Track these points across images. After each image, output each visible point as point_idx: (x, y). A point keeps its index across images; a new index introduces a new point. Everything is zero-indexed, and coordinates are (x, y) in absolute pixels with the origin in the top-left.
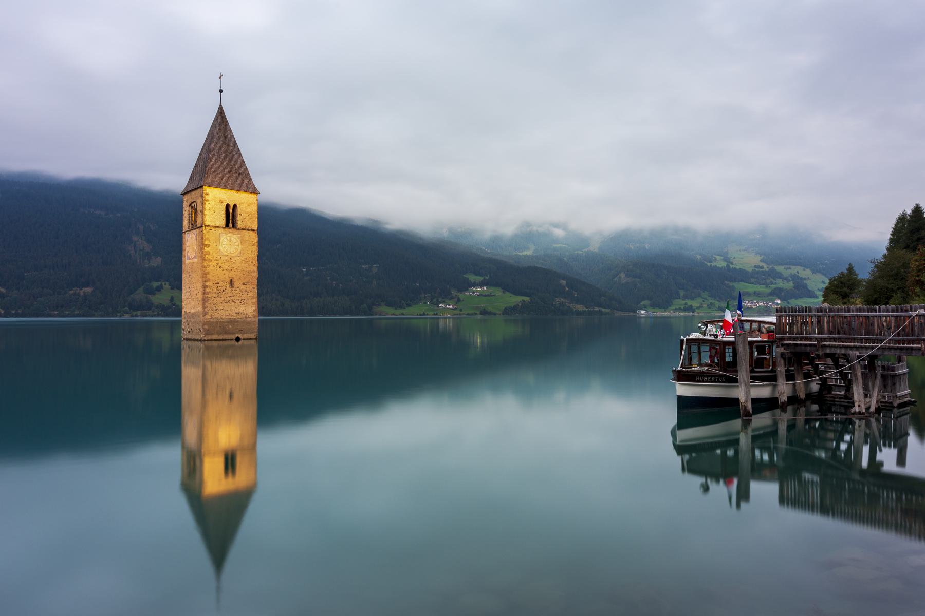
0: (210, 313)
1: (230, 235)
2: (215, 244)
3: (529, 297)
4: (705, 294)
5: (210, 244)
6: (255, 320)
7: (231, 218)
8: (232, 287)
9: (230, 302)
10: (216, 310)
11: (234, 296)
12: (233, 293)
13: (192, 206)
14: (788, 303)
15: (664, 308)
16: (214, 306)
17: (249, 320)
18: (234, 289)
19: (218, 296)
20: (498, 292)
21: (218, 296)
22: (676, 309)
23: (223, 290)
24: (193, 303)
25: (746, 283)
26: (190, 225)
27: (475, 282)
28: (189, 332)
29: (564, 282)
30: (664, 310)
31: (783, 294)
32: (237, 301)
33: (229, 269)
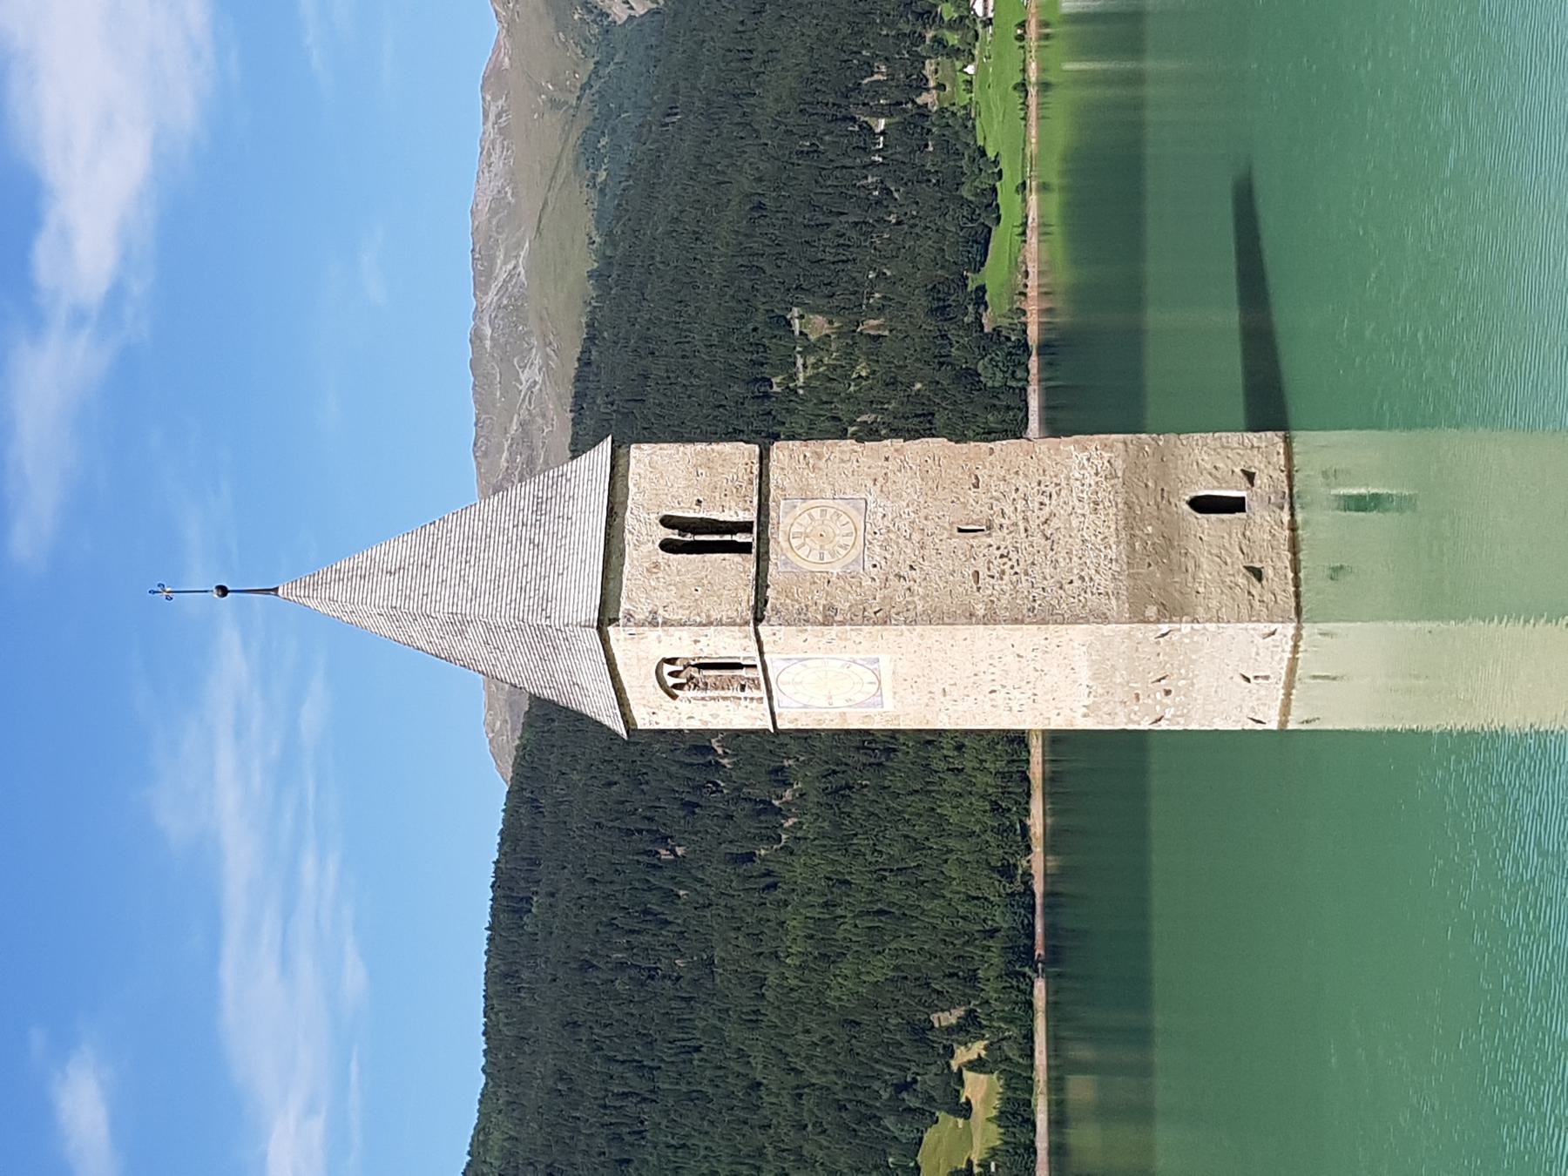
0: (1094, 601)
2: (822, 584)
5: (823, 602)
6: (1121, 446)
7: (716, 538)
8: (989, 528)
9: (1048, 534)
10: (1082, 578)
11: (1026, 519)
12: (1015, 524)
16: (1067, 587)
17: (1119, 464)
18: (997, 521)
19: (1026, 574)
21: (1026, 574)
23: (1002, 556)
32: (1047, 510)
33: (916, 537)
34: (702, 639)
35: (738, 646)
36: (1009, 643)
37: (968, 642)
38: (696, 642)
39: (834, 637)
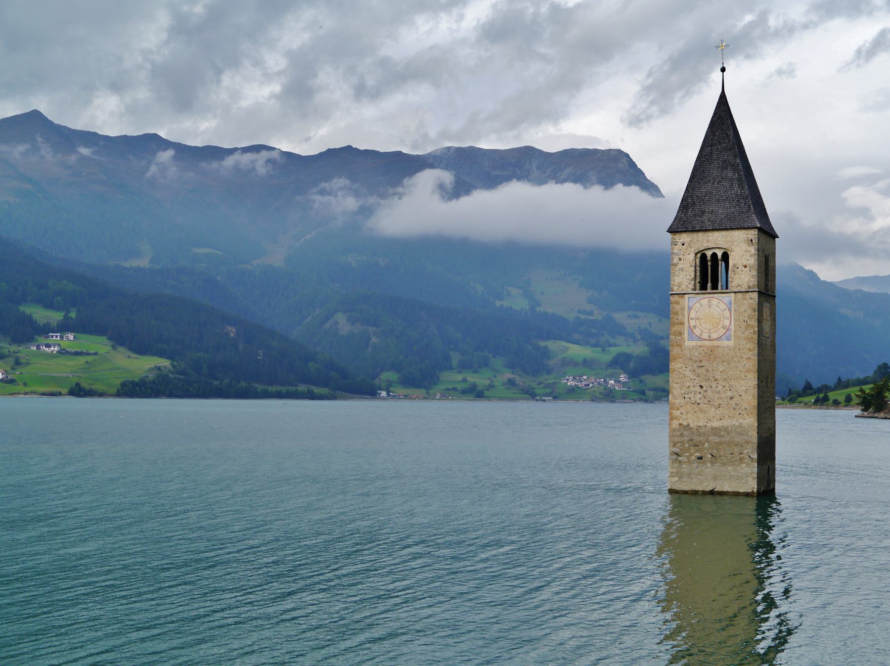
1: (766, 304)
3: (167, 358)
4: (498, 362)
13: (703, 257)
14: (641, 381)
15: (426, 388)
20: (99, 344)
22: (447, 389)
24: (712, 412)
25: (568, 341)
26: (698, 285)
27: (48, 323)
28: (700, 458)
29: (232, 331)
30: (422, 392)
31: (632, 364)
34: (747, 269)
35: (741, 283)
36: (743, 394)
37: (743, 375)
38: (745, 267)
39: (748, 323)
